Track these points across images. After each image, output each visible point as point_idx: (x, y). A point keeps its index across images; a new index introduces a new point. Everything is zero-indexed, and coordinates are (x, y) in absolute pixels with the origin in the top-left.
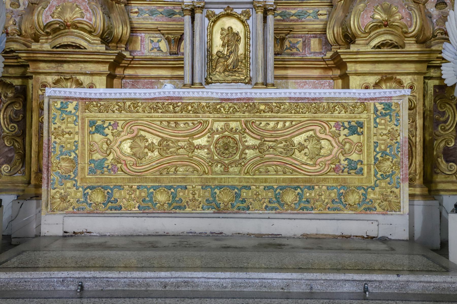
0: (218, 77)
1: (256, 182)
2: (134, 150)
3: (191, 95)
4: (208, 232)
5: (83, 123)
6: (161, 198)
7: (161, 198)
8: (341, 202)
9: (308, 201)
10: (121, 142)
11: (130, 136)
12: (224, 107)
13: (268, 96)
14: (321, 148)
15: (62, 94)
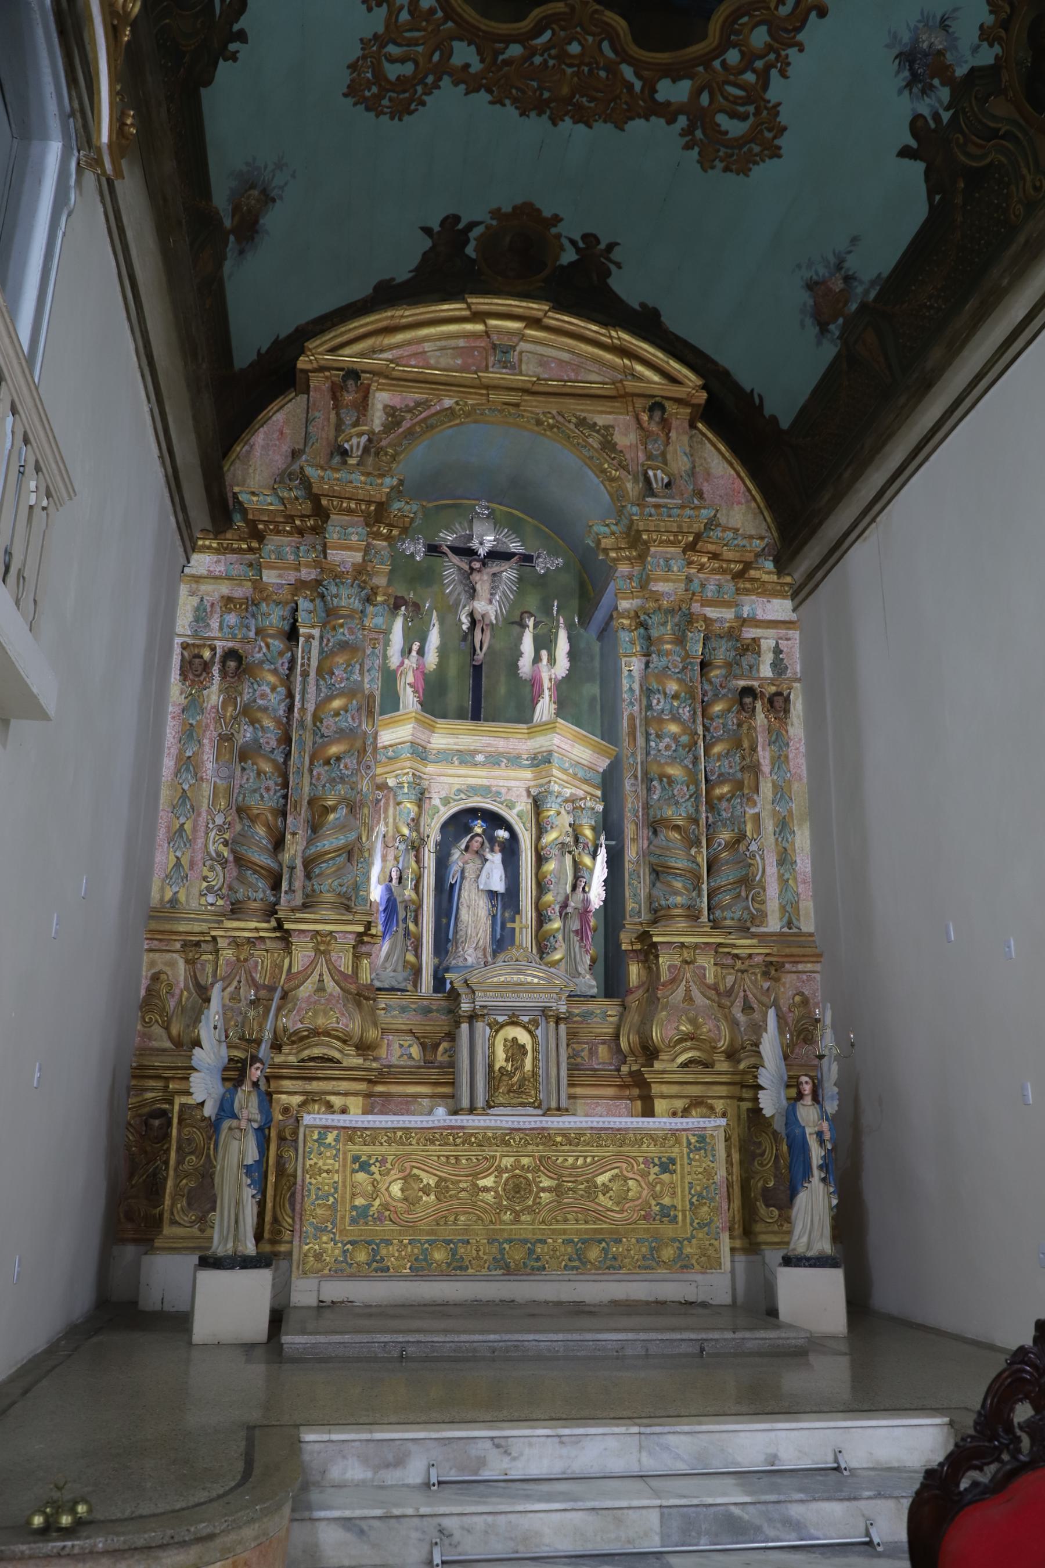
0: (501, 1100)
1: (553, 1234)
2: (406, 1193)
3: (476, 1124)
4: (497, 1300)
5: (345, 1159)
6: (439, 1255)
7: (439, 1255)
8: (653, 1259)
9: (615, 1258)
10: (390, 1184)
11: (401, 1175)
12: (514, 1139)
13: (567, 1125)
14: (629, 1190)
15: (324, 1123)
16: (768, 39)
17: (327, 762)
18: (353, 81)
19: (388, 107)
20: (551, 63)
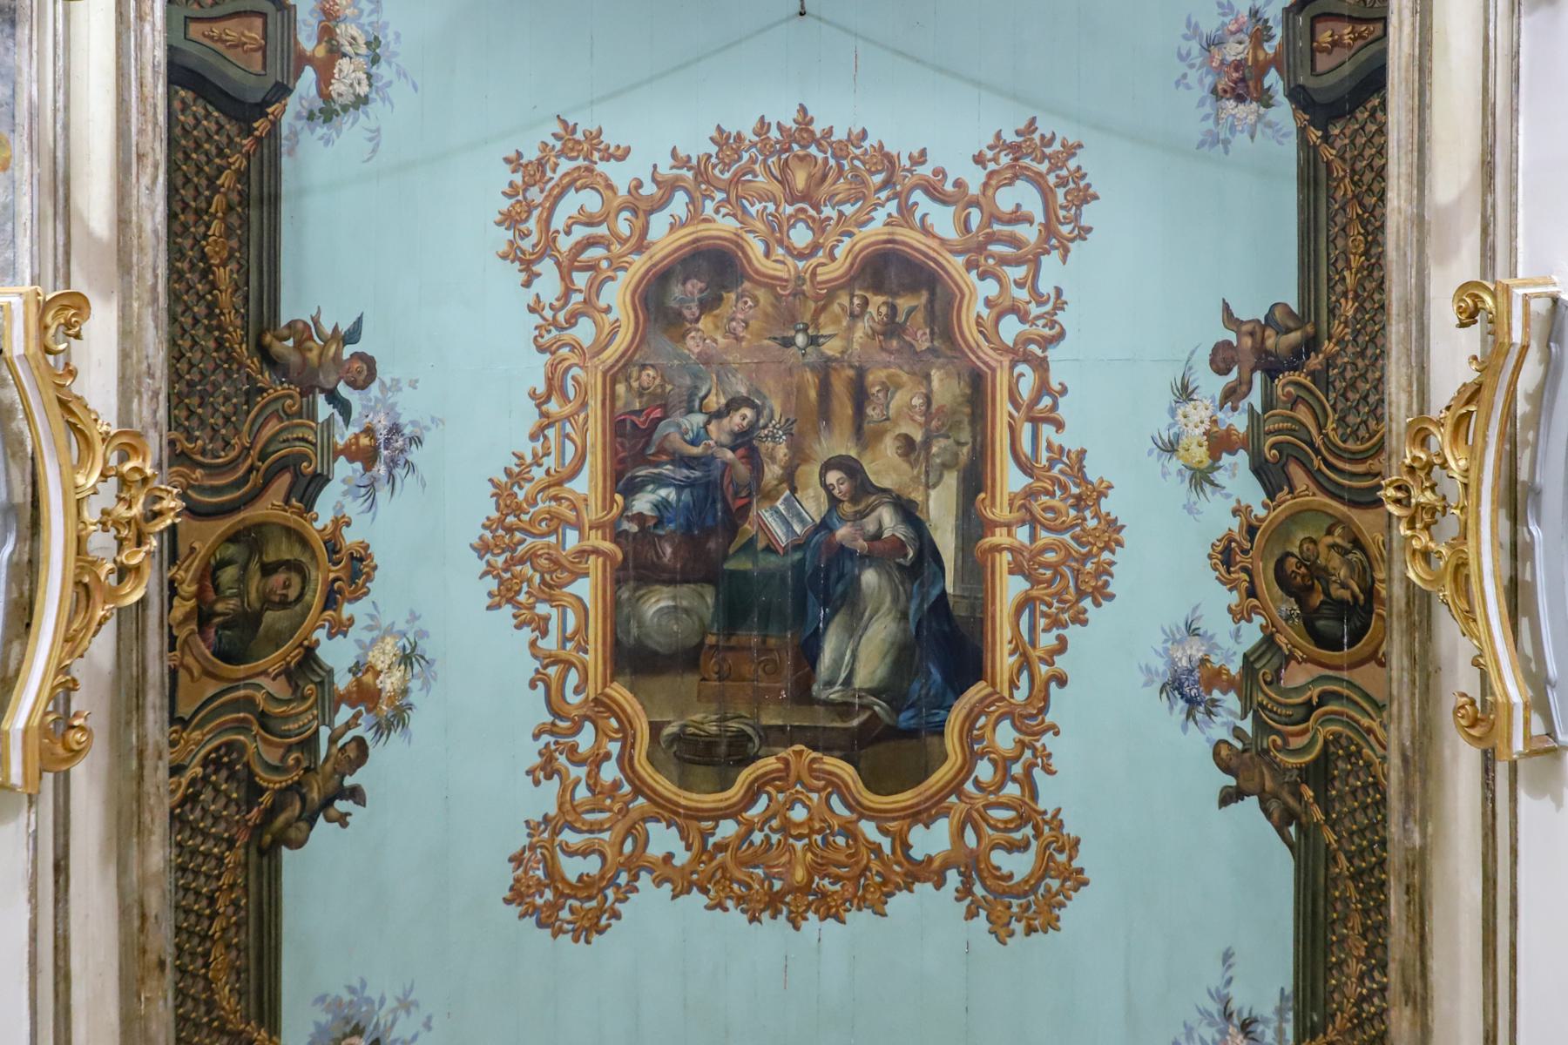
16: (1016, 735)
18: (517, 880)
19: (569, 922)
20: (775, 838)
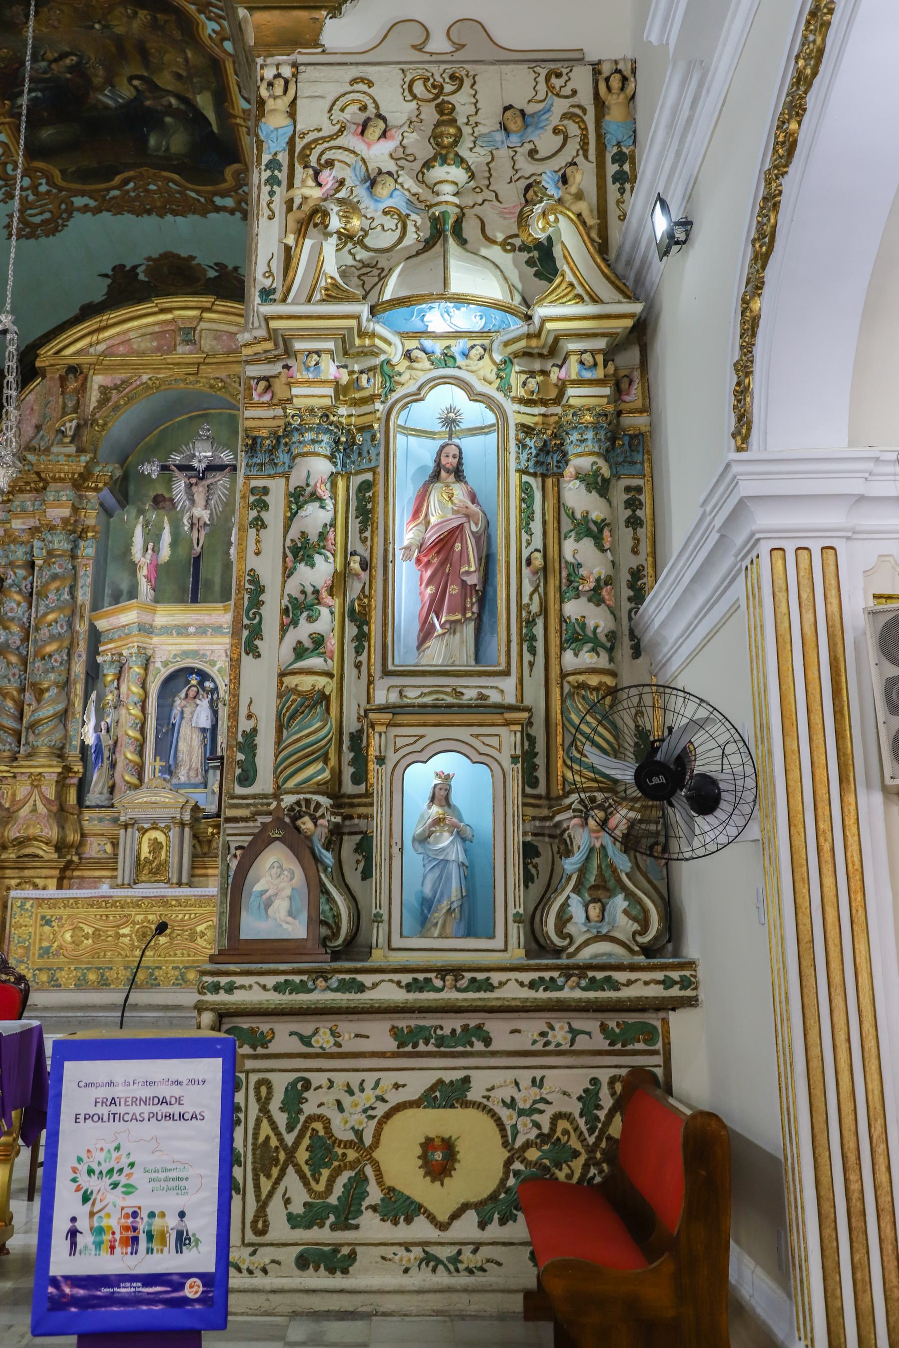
0: (144, 878)
6: (92, 977)
7: (92, 977)
17: (43, 658)
